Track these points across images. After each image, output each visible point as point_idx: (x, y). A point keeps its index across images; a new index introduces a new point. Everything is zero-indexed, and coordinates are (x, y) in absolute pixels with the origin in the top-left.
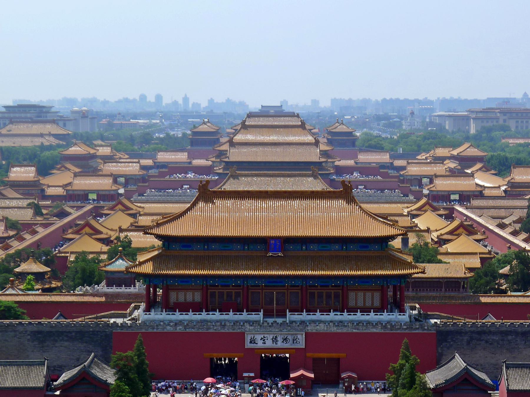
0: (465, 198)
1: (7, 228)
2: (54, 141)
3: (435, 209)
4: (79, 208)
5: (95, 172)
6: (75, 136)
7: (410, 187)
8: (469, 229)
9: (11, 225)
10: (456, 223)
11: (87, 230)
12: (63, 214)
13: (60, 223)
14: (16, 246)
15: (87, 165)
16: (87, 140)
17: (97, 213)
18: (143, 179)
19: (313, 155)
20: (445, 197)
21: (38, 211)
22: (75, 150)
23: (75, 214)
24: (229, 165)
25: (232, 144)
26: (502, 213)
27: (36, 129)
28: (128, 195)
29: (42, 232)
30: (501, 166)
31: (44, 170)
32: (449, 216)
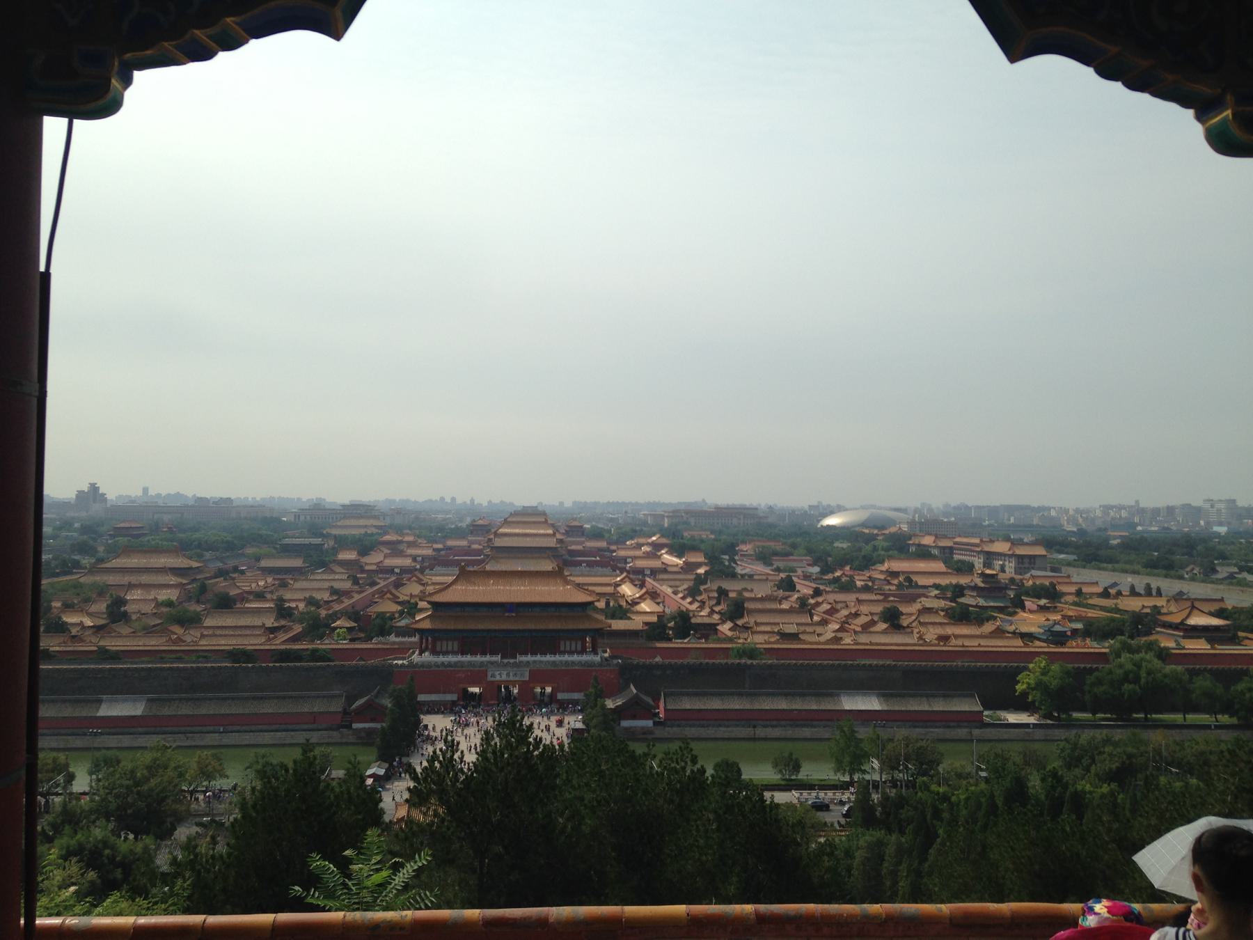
0: (654, 572)
1: (331, 594)
2: (375, 531)
3: (632, 581)
4: (386, 579)
5: (401, 554)
6: (391, 526)
7: (615, 565)
8: (654, 595)
9: (334, 592)
10: (644, 590)
11: (388, 595)
12: (374, 584)
13: (370, 590)
14: (337, 607)
15: (395, 549)
16: (399, 530)
17: (398, 585)
18: (435, 559)
19: (551, 543)
20: (640, 572)
21: (356, 581)
22: (387, 538)
23: (382, 583)
24: (493, 548)
25: (496, 534)
26: (678, 583)
27: (362, 522)
28: (422, 571)
29: (357, 597)
30: (679, 551)
31: (364, 551)
32: (642, 586)
